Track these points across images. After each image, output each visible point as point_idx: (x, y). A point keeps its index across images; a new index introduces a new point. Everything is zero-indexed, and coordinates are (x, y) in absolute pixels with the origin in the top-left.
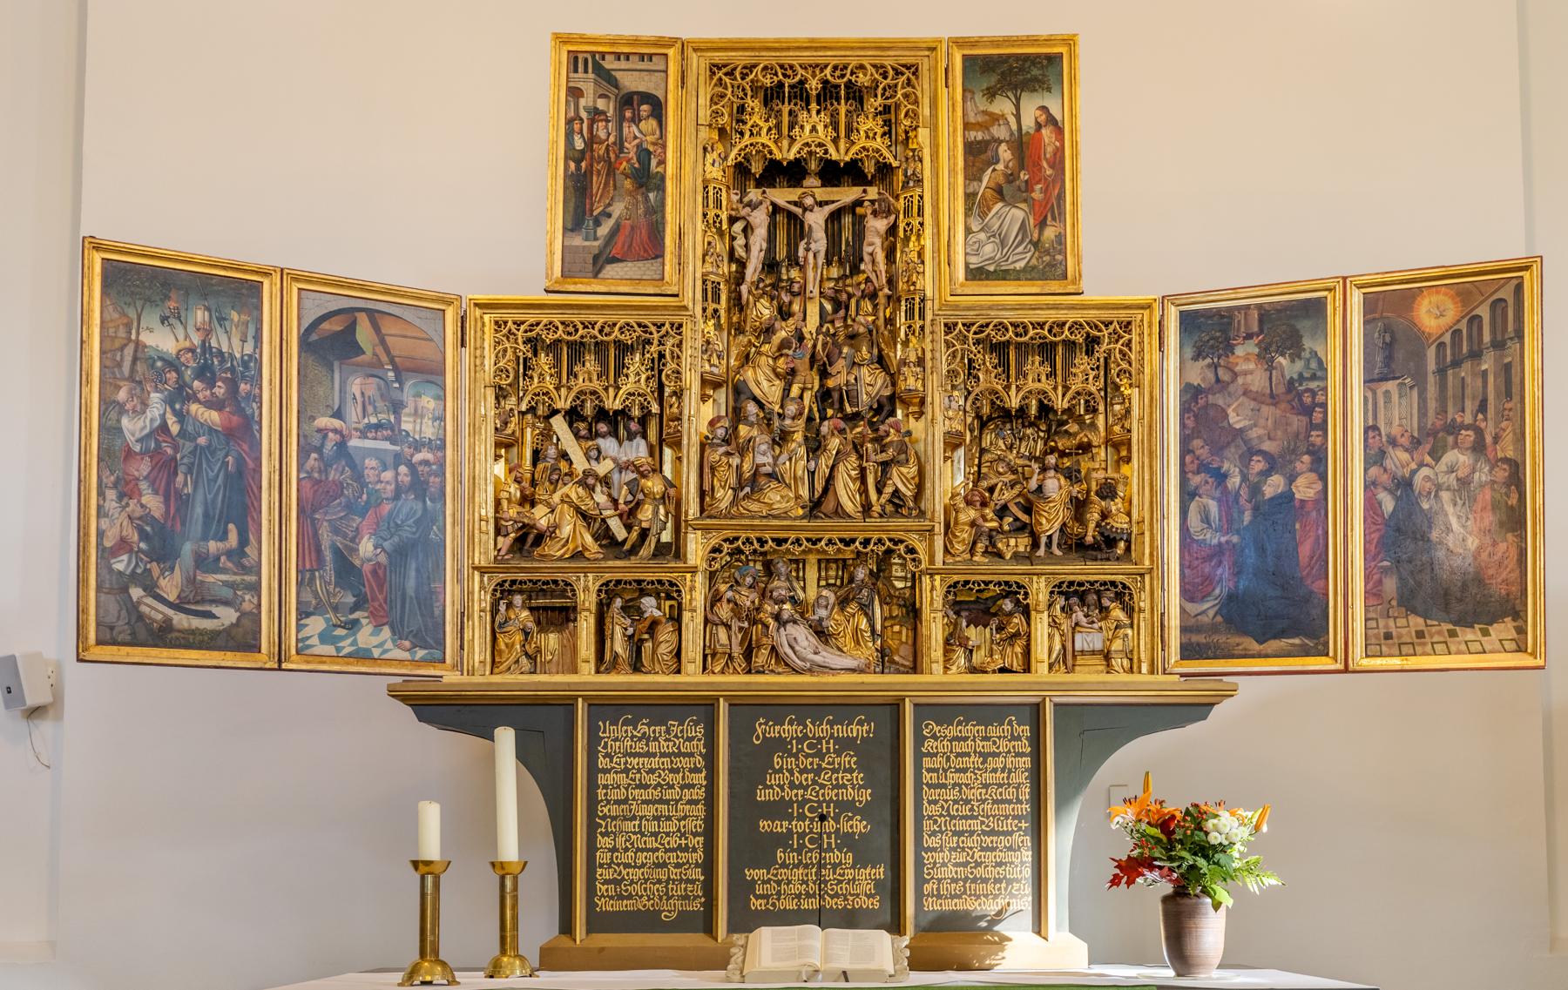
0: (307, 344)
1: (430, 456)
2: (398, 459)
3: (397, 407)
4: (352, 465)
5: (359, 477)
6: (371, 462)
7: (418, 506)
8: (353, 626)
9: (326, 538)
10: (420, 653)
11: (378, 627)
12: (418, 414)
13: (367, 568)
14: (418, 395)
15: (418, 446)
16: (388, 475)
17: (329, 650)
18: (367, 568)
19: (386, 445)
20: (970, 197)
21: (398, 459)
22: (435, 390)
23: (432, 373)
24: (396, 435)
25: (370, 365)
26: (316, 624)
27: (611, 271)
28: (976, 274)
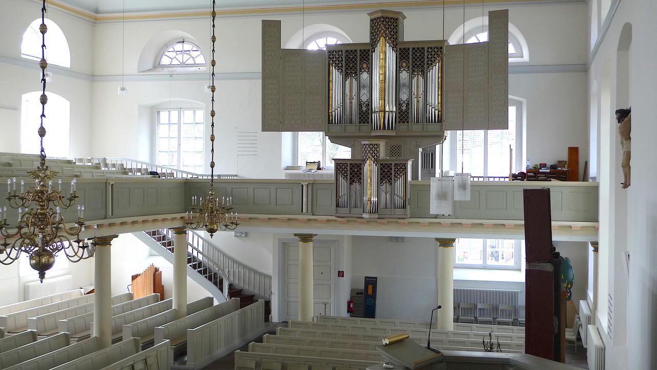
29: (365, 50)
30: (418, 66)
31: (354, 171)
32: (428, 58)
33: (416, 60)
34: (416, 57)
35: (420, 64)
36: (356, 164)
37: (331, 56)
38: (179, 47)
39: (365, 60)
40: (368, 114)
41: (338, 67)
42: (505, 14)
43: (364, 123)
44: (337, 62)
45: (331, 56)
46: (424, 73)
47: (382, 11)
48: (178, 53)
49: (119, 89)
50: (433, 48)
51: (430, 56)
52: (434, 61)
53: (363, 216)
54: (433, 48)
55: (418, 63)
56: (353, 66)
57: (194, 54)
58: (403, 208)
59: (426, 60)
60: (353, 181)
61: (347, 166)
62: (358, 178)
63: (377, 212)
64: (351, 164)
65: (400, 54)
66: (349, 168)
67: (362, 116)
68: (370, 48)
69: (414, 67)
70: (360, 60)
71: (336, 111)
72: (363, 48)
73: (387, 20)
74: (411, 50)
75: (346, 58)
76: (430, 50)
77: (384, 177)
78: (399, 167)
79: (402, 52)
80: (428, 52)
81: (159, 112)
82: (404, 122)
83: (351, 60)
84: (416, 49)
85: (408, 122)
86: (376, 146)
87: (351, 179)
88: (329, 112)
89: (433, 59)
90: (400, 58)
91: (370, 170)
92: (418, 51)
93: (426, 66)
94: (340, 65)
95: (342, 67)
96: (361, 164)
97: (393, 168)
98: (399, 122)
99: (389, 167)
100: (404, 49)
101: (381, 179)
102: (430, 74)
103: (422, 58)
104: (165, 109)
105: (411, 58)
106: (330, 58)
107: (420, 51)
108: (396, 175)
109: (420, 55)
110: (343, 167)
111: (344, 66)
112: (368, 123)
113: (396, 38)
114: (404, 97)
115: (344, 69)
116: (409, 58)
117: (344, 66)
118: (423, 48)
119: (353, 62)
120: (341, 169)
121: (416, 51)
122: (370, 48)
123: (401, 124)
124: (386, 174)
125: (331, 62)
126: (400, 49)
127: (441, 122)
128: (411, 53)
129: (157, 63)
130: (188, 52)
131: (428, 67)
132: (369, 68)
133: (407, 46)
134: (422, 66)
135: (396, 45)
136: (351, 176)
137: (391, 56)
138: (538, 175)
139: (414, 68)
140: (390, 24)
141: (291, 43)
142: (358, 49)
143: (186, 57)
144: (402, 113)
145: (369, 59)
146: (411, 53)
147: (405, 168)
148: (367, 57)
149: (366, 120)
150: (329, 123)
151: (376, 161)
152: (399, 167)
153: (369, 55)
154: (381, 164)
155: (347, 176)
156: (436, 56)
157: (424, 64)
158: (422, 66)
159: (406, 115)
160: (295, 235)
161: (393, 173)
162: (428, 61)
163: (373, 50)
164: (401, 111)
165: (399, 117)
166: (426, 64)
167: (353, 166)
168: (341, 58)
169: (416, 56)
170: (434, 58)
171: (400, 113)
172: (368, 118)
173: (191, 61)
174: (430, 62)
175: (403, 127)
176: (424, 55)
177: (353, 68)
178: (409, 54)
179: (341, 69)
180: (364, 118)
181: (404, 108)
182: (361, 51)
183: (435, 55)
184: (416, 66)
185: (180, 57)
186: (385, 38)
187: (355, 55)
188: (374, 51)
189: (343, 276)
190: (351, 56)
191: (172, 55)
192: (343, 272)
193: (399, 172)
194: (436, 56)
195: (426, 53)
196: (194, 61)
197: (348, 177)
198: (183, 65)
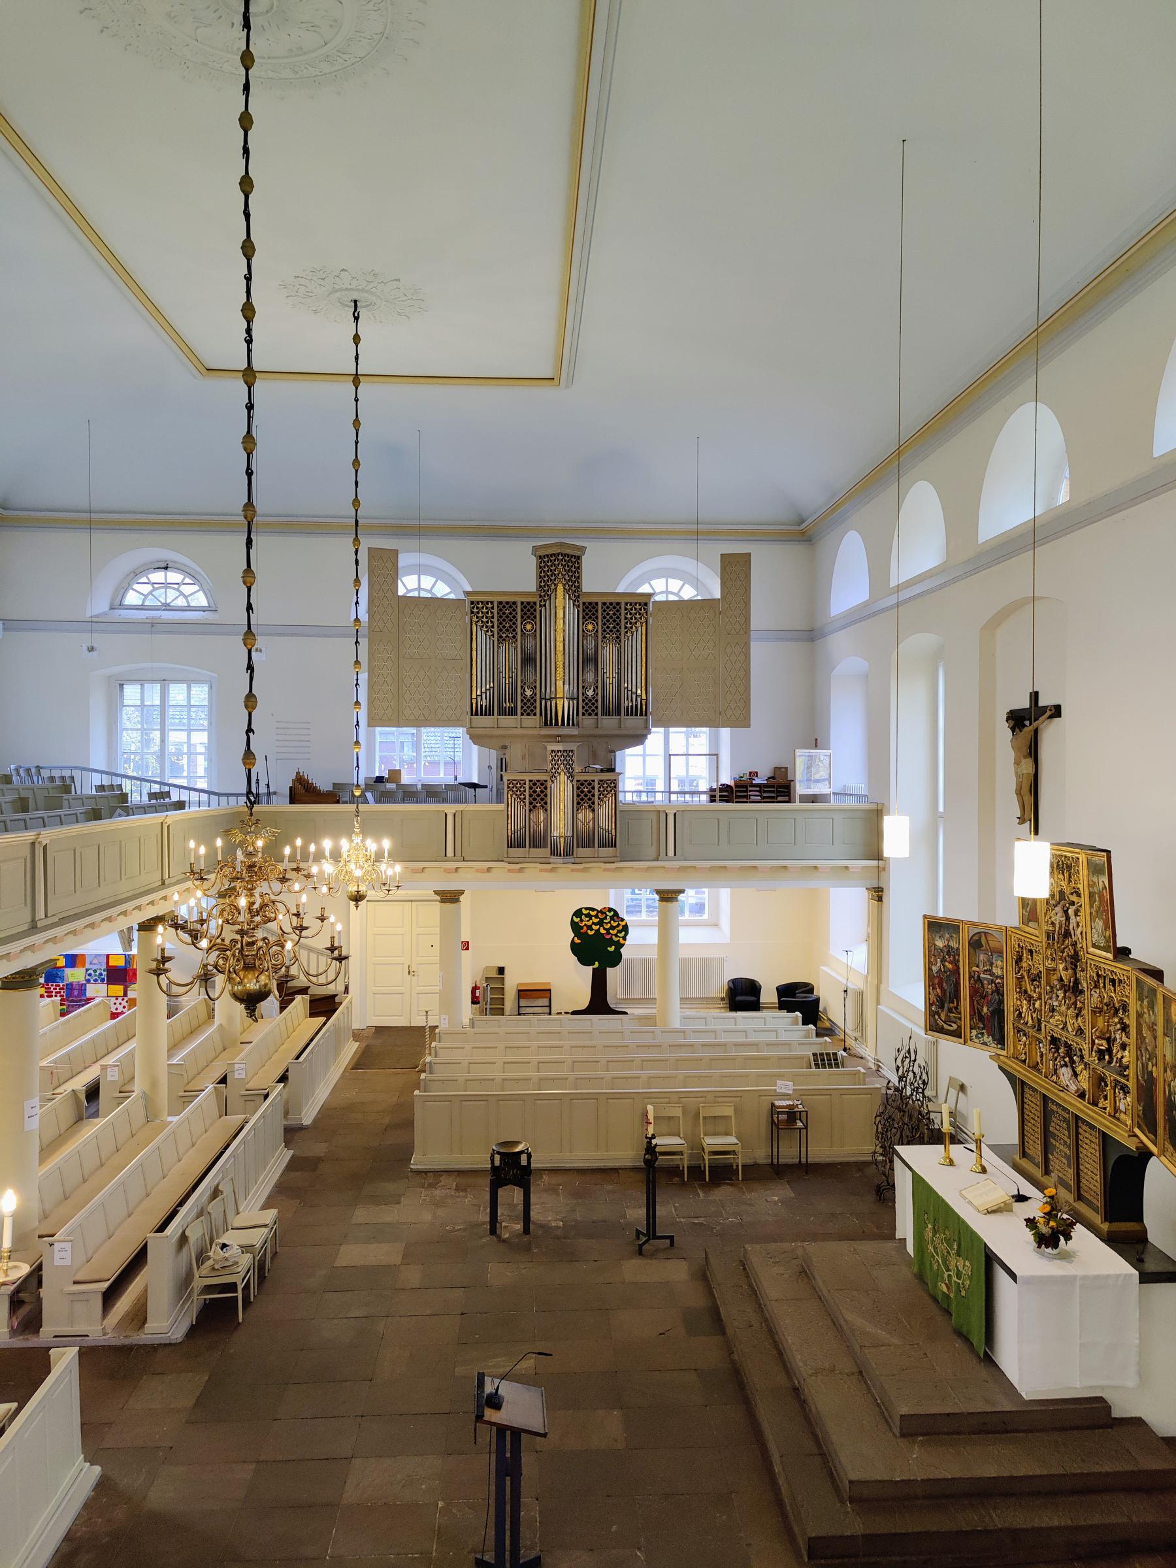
0: (969, 942)
1: (1000, 981)
2: (993, 981)
3: (992, 964)
4: (981, 981)
5: (982, 985)
6: (986, 982)
7: (997, 997)
8: (982, 1034)
9: (975, 1003)
10: (999, 1046)
11: (989, 1035)
12: (997, 967)
13: (986, 1016)
14: (997, 960)
15: (997, 977)
16: (990, 987)
17: (977, 1041)
18: (986, 1016)
19: (989, 977)
20: (1091, 913)
21: (993, 981)
22: (1001, 959)
23: (1000, 953)
24: (992, 974)
25: (984, 950)
26: (974, 1032)
27: (1031, 924)
28: (1094, 946)
29: (528, 603)
30: (611, 631)
31: (535, 792)
32: (626, 618)
33: (608, 621)
34: (608, 617)
35: (614, 627)
36: (538, 781)
37: (475, 610)
38: (158, 577)
39: (529, 617)
40: (535, 701)
41: (487, 627)
42: (744, 560)
43: (528, 714)
44: (485, 620)
45: (475, 610)
46: (620, 641)
47: (561, 545)
48: (156, 586)
49: (85, 648)
50: (633, 604)
51: (629, 616)
52: (636, 623)
53: (551, 860)
54: (633, 604)
55: (611, 626)
56: (511, 627)
57: (186, 590)
58: (612, 847)
59: (623, 621)
60: (534, 807)
61: (525, 784)
62: (542, 802)
63: (573, 854)
64: (530, 781)
65: (584, 611)
66: (527, 786)
67: (525, 704)
68: (537, 599)
69: (604, 631)
70: (522, 617)
71: (484, 696)
72: (525, 599)
73: (567, 559)
74: (600, 605)
75: (498, 613)
76: (629, 607)
77: (582, 799)
78: (605, 785)
79: (587, 608)
80: (626, 609)
81: (121, 686)
82: (590, 714)
83: (507, 617)
84: (608, 604)
85: (596, 714)
86: (571, 754)
87: (531, 803)
88: (471, 699)
89: (633, 621)
90: (584, 617)
91: (562, 791)
92: (611, 607)
93: (623, 630)
94: (490, 624)
95: (493, 627)
96: (546, 781)
97: (597, 786)
98: (584, 714)
99: (589, 784)
100: (590, 604)
101: (578, 803)
103: (618, 618)
104: (132, 681)
105: (600, 617)
106: (472, 612)
107: (614, 608)
108: (602, 796)
109: (614, 614)
110: (518, 785)
111: (496, 626)
112: (535, 714)
113: (579, 587)
114: (590, 677)
115: (495, 630)
116: (597, 618)
117: (496, 626)
118: (618, 604)
119: (511, 620)
120: (514, 789)
121: (608, 607)
122: (537, 599)
124: (586, 796)
125: (475, 619)
126: (584, 604)
127: (646, 715)
128: (600, 611)
129: (117, 602)
130: (176, 586)
131: (627, 632)
132: (535, 631)
133: (594, 600)
134: (618, 631)
135: (578, 597)
136: (531, 798)
137: (573, 613)
138: (750, 789)
139: (605, 633)
140: (570, 564)
141: (408, 585)
142: (519, 599)
143: (172, 594)
144: (587, 701)
145: (535, 617)
146: (600, 611)
147: (615, 787)
148: (532, 614)
149: (532, 711)
150: (472, 715)
151: (571, 776)
152: (605, 785)
153: (535, 610)
154: (578, 781)
155: (525, 799)
156: (638, 616)
157: (620, 628)
158: (618, 631)
159: (593, 704)
160: (436, 892)
161: (597, 793)
162: (627, 623)
163: (543, 603)
164: (586, 698)
165: (583, 707)
166: (623, 627)
167: (535, 784)
168: (492, 613)
169: (608, 614)
170: (636, 618)
171: (583, 701)
172: (535, 707)
173: (181, 602)
174: (628, 625)
175: (587, 721)
176: (620, 614)
178: (597, 611)
179: (492, 631)
181: (590, 693)
182: (522, 603)
183: (636, 614)
184: (608, 630)
185: (160, 593)
186: (564, 585)
187: (514, 610)
188: (545, 605)
189: (467, 949)
190: (507, 612)
191: (146, 589)
192: (468, 942)
193: (605, 793)
194: (638, 616)
195: (623, 612)
196: (188, 602)
197: (527, 801)
198: (167, 607)
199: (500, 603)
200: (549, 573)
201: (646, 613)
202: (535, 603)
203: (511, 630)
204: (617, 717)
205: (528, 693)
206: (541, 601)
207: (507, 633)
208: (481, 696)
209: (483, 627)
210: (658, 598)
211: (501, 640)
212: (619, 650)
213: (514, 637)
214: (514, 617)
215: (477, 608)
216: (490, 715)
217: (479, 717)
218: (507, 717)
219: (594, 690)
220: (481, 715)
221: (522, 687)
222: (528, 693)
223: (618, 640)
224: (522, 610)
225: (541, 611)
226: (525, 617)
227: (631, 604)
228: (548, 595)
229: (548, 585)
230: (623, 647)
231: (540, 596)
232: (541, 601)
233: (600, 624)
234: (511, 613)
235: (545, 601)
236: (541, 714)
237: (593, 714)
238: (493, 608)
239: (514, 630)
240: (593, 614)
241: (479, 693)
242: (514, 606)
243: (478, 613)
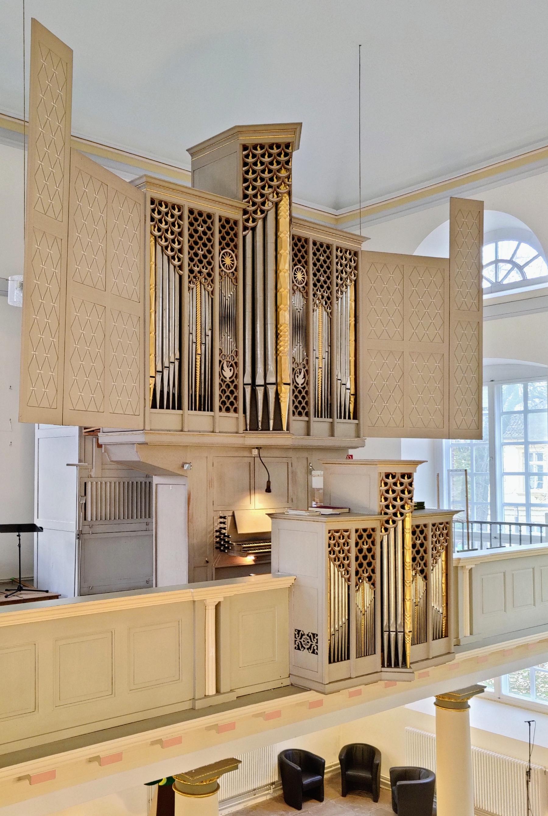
29: (228, 221)
40: (236, 387)
43: (228, 410)
54: (344, 251)
70: (220, 243)
85: (307, 414)
95: (180, 251)
102: (337, 306)
106: (152, 219)
112: (236, 410)
115: (185, 257)
116: (306, 262)
119: (205, 245)
123: (297, 417)
127: (355, 418)
145: (236, 246)
149: (232, 404)
153: (236, 235)
163: (250, 224)
172: (236, 398)
177: (205, 261)
180: (228, 398)
181: (300, 380)
187: (209, 229)
188: (254, 229)
190: (200, 229)
199: (191, 212)
200: (266, 175)
201: (356, 268)
202: (236, 223)
203: (205, 261)
204: (326, 420)
205: (228, 373)
206: (247, 220)
207: (201, 266)
208: (162, 372)
209: (167, 248)
210: (365, 247)
211: (192, 276)
212: (330, 315)
213: (209, 275)
214: (209, 240)
215: (159, 213)
216: (174, 408)
217: (158, 410)
218: (198, 412)
219: (304, 377)
220: (161, 407)
221: (220, 361)
222: (228, 373)
223: (329, 302)
224: (220, 232)
225: (244, 237)
226: (224, 243)
227: (341, 252)
228: (262, 212)
229: (262, 196)
230: (335, 314)
231: (245, 212)
232: (247, 220)
233: (311, 272)
234: (205, 233)
235: (254, 221)
236: (245, 412)
237: (304, 414)
238: (180, 217)
239: (209, 263)
240: (303, 257)
241: (159, 368)
242: (209, 221)
243: (160, 221)
